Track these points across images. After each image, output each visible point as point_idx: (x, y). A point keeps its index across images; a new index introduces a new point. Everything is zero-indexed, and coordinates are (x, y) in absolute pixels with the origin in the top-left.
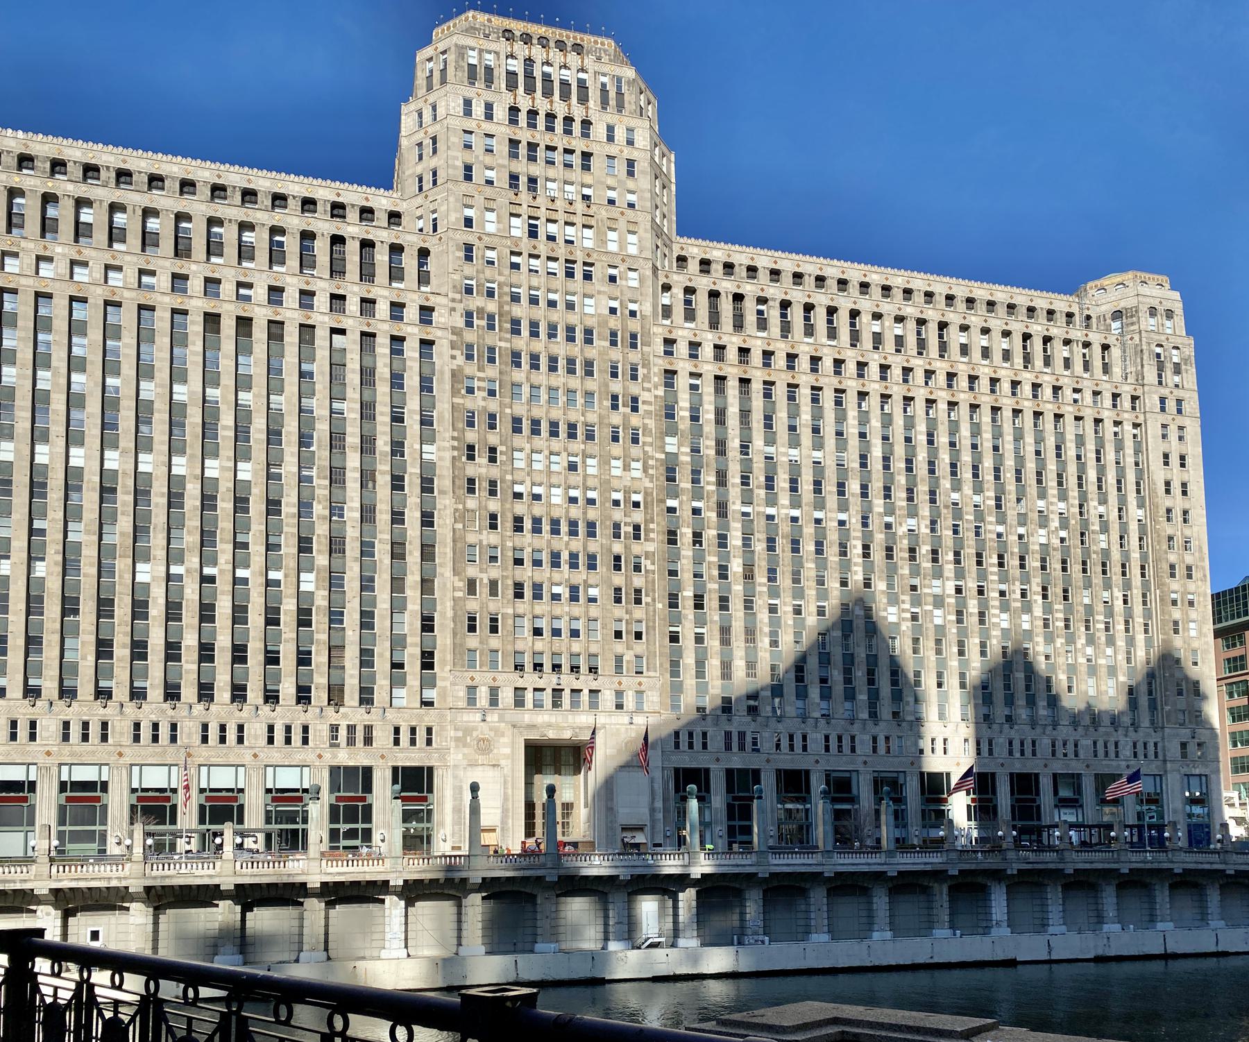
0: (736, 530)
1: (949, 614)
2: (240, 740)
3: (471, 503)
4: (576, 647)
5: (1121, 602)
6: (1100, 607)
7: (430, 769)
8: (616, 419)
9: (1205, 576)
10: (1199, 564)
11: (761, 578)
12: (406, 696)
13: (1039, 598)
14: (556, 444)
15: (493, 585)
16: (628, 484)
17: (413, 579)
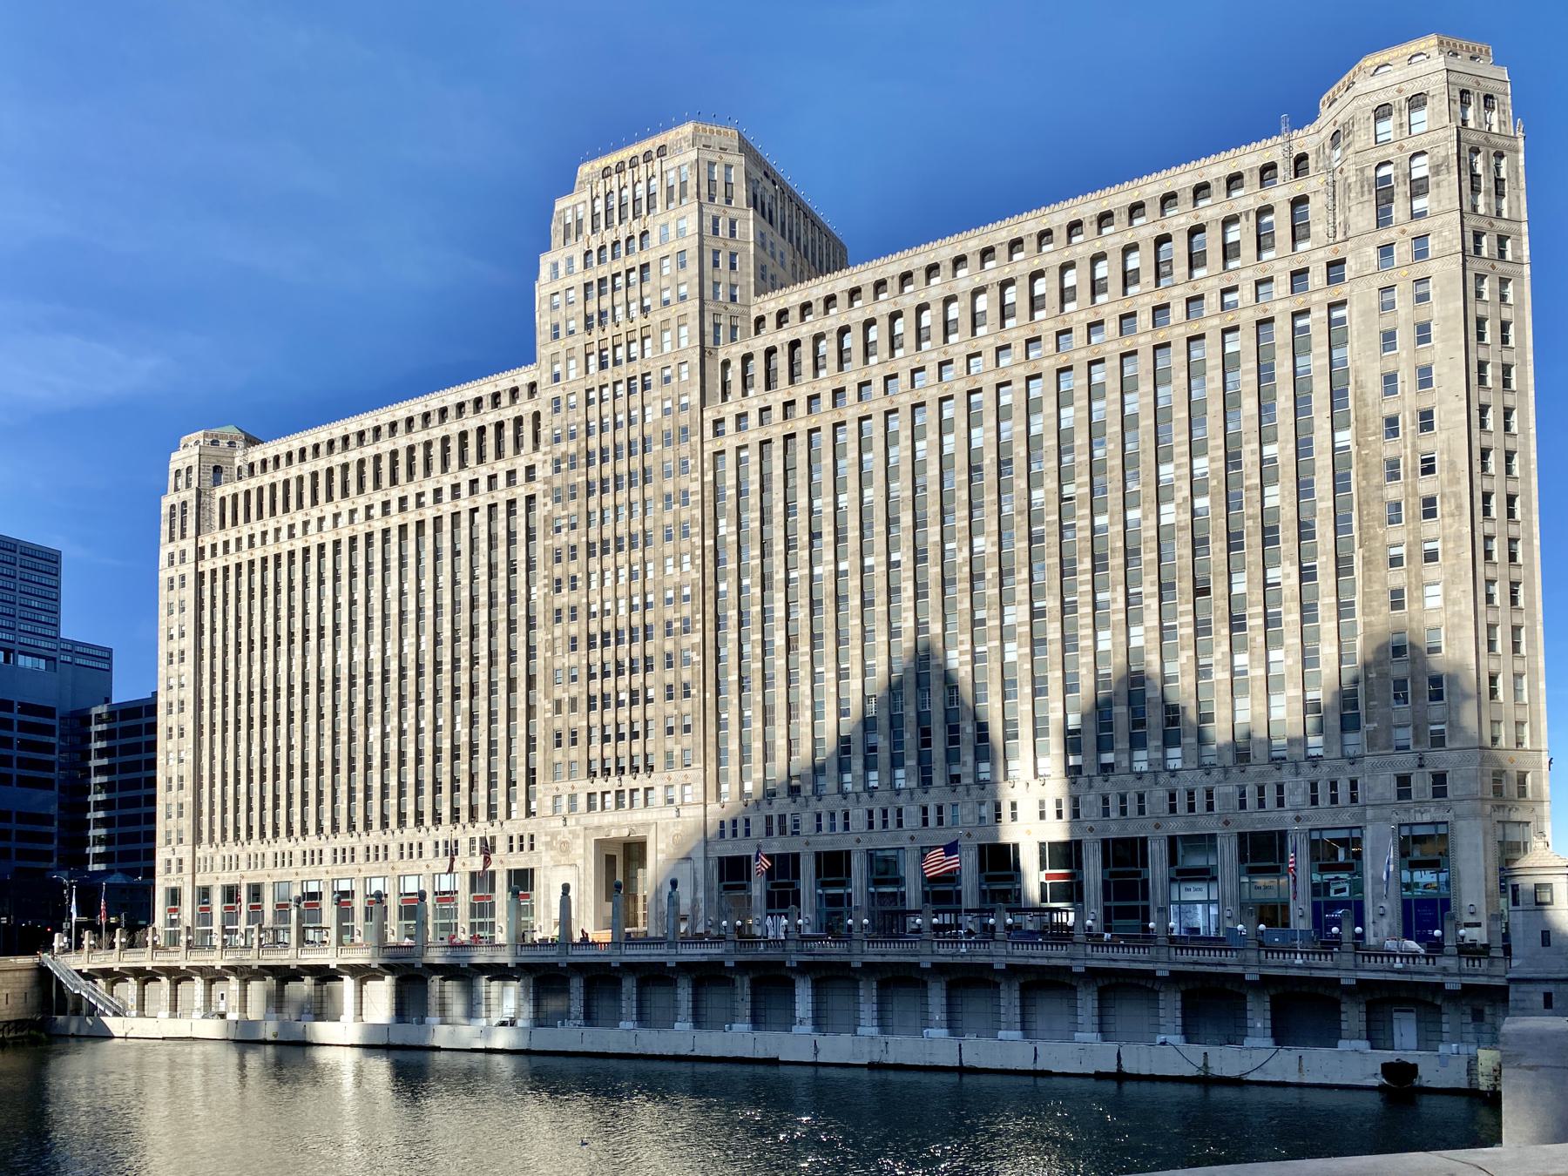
0: (779, 600)
1: (1020, 646)
2: (420, 854)
3: (558, 631)
4: (637, 747)
5: (1295, 579)
6: (1258, 595)
7: (532, 870)
8: (668, 519)
9: (1459, 507)
10: (1447, 490)
11: (804, 647)
12: (518, 808)
13: (1154, 603)
14: (622, 558)
15: (573, 703)
16: (678, 579)
17: (521, 707)
